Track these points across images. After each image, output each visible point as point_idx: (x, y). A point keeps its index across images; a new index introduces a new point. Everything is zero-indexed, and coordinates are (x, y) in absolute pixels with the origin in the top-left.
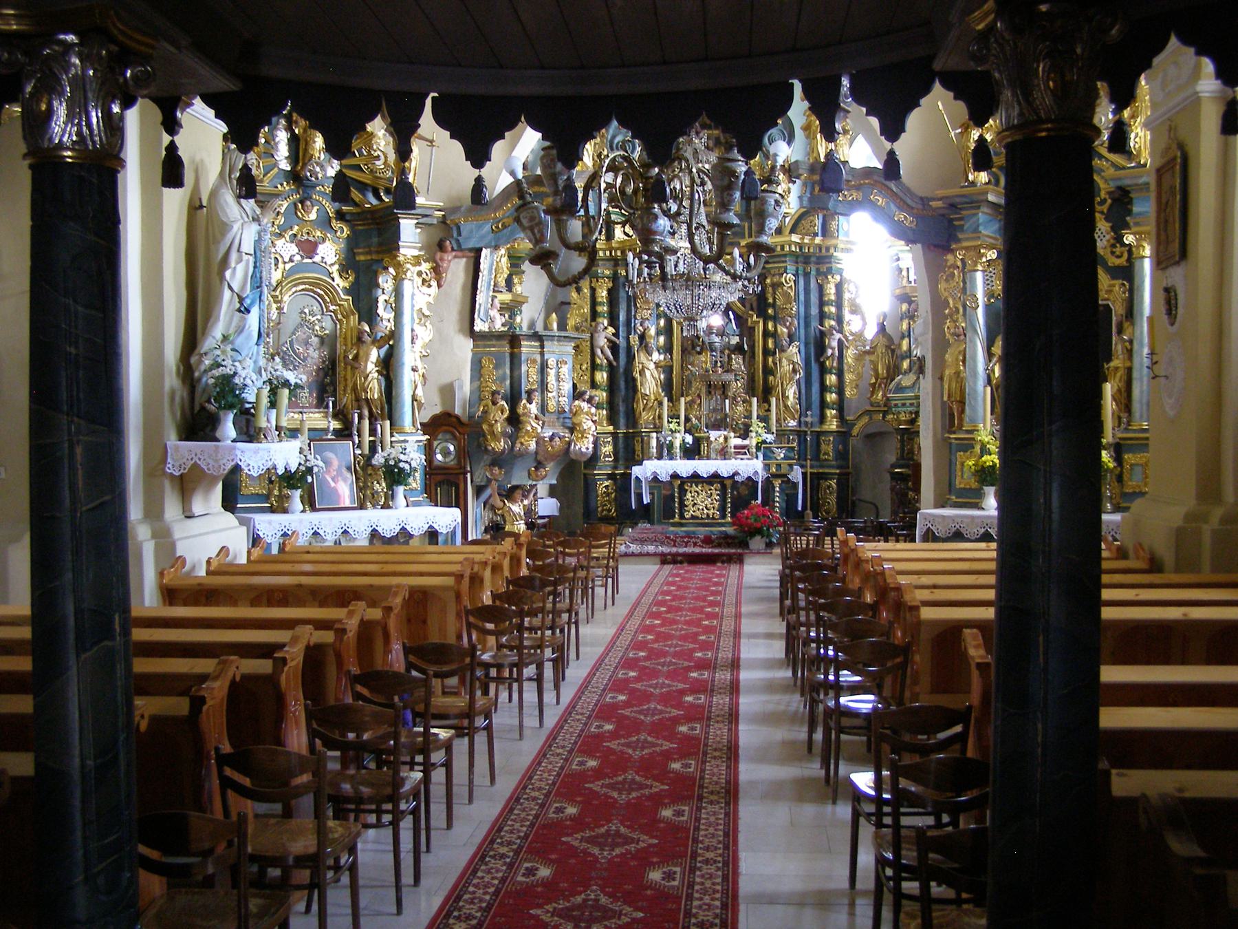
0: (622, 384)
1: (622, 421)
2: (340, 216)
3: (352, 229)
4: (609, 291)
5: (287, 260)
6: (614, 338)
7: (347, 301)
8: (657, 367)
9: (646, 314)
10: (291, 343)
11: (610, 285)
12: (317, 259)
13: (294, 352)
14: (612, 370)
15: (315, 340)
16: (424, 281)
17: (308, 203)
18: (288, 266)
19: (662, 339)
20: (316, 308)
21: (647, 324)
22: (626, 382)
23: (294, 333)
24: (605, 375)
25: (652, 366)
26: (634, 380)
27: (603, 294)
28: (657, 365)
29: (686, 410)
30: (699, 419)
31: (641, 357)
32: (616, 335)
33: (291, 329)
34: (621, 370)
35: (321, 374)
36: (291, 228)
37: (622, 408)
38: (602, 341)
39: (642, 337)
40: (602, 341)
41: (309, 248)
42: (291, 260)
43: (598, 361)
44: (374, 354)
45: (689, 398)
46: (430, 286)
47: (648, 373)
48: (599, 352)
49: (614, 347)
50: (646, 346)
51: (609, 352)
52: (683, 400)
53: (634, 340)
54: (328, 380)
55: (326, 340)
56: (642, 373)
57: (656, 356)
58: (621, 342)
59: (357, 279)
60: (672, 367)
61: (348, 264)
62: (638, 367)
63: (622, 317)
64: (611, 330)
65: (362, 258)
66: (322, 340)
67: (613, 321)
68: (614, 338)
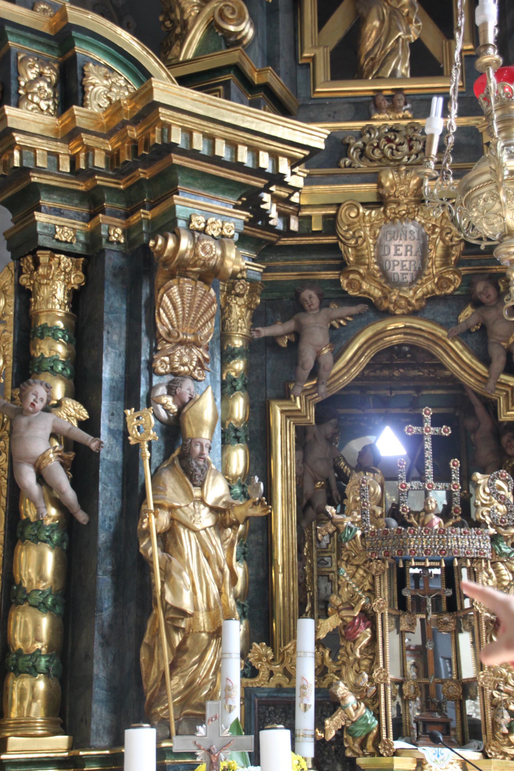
0: (104, 584)
1: (99, 714)
4: (76, 298)
6: (84, 437)
8: (220, 525)
9: (186, 359)
11: (76, 279)
14: (74, 541)
19: (238, 459)
21: (187, 387)
22: (117, 574)
24: (50, 558)
25: (205, 519)
26: (144, 565)
27: (55, 299)
28: (222, 518)
29: (321, 672)
30: (372, 702)
31: (167, 496)
32: (90, 426)
34: (103, 537)
37: (99, 670)
38: (39, 441)
39: (174, 431)
40: (39, 441)
43: (29, 512)
45: (330, 623)
47: (188, 542)
48: (29, 477)
49: (81, 463)
50: (185, 458)
51: (62, 479)
52: (307, 630)
53: (145, 427)
56: (168, 539)
57: (216, 490)
58: (107, 448)
60: (265, 524)
62: (155, 522)
63: (110, 370)
64: (74, 411)
67: (83, 385)
68: (84, 437)
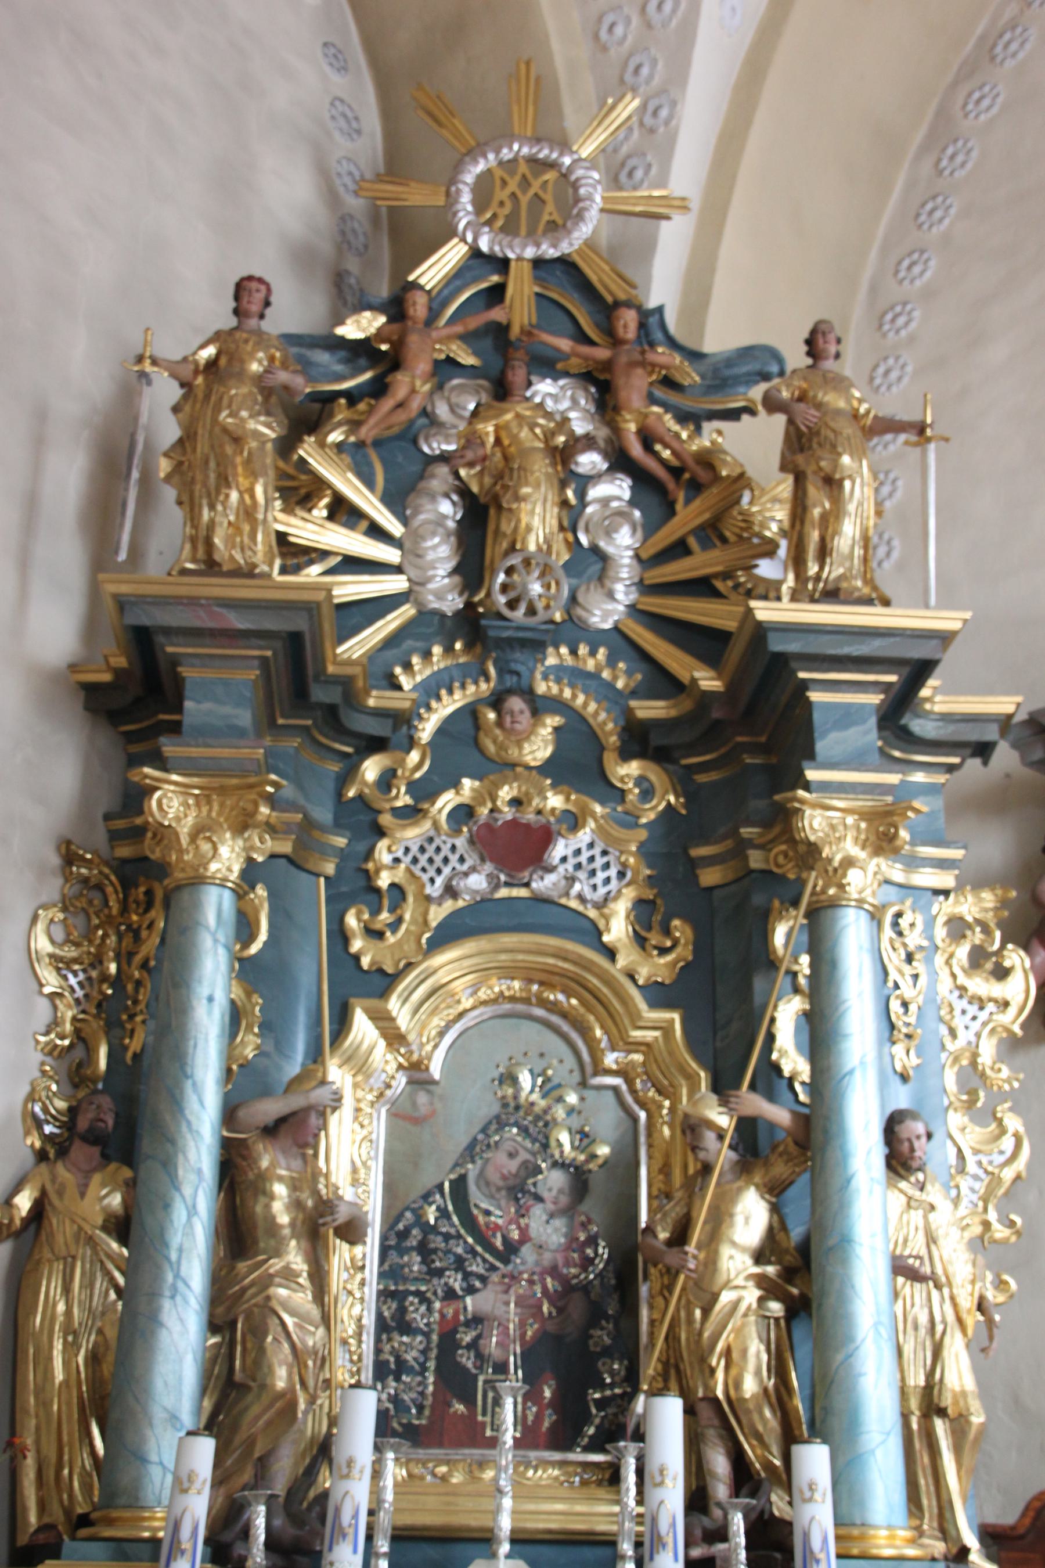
2: (638, 740)
3: (683, 783)
5: (435, 890)
7: (661, 1024)
10: (460, 1186)
12: (545, 884)
13: (469, 1222)
15: (553, 1182)
16: (978, 958)
17: (516, 703)
18: (437, 915)
20: (562, 1066)
23: (470, 1152)
33: (464, 1141)
35: (577, 1308)
36: (456, 785)
41: (519, 846)
42: (450, 891)
44: (751, 1216)
46: (1001, 973)
54: (603, 1336)
55: (597, 1183)
59: (702, 945)
61: (670, 891)
65: (709, 877)
66: (580, 1181)
